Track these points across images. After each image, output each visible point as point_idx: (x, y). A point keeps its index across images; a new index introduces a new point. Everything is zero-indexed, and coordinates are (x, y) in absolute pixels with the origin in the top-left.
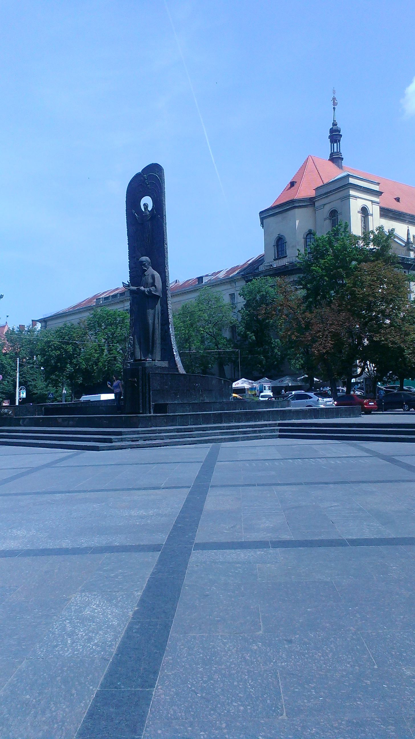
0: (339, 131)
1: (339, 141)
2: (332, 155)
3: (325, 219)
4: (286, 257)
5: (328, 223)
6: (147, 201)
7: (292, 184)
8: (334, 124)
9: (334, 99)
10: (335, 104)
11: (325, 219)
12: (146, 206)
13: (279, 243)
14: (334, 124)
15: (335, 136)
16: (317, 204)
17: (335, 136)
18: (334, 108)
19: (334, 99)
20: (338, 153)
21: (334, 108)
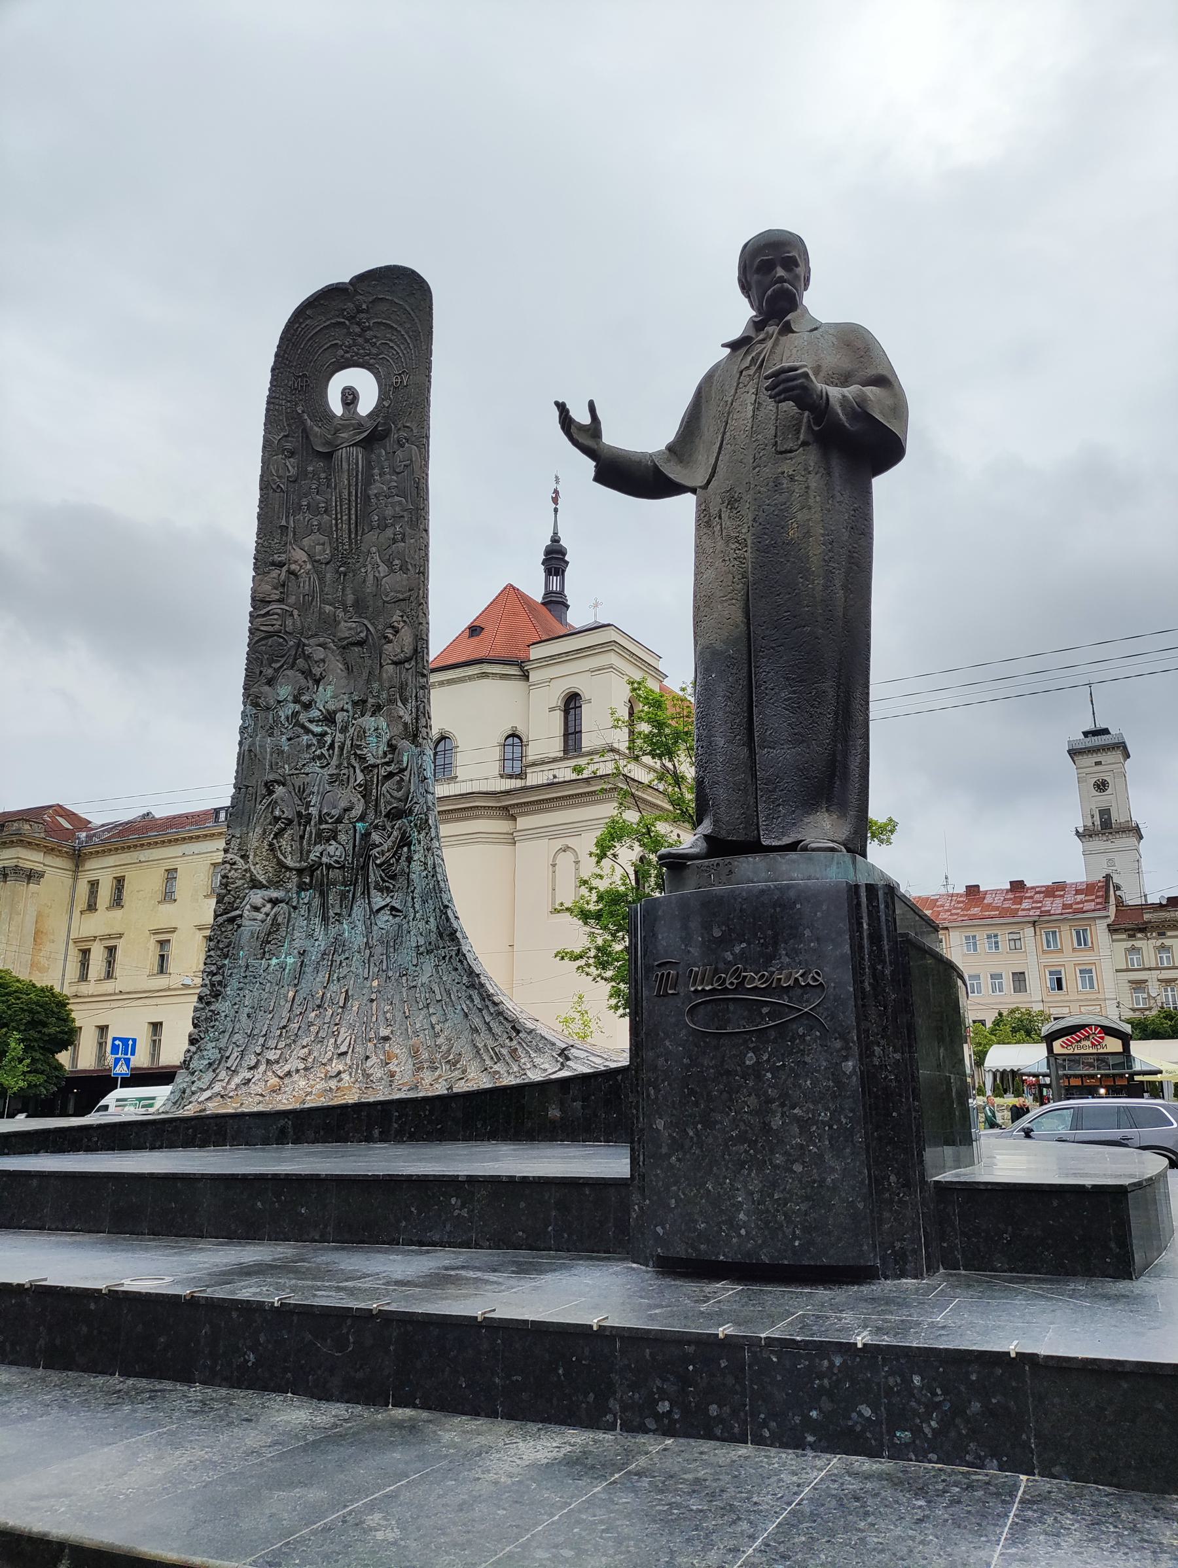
0: (564, 554)
1: (563, 571)
2: (548, 593)
3: (552, 709)
5: (559, 716)
6: (357, 387)
7: (474, 630)
8: (555, 540)
9: (556, 492)
10: (555, 500)
11: (552, 709)
12: (350, 397)
13: (441, 747)
14: (555, 540)
15: (555, 560)
16: (533, 676)
17: (555, 560)
18: (556, 510)
19: (556, 492)
20: (561, 593)
21: (556, 510)
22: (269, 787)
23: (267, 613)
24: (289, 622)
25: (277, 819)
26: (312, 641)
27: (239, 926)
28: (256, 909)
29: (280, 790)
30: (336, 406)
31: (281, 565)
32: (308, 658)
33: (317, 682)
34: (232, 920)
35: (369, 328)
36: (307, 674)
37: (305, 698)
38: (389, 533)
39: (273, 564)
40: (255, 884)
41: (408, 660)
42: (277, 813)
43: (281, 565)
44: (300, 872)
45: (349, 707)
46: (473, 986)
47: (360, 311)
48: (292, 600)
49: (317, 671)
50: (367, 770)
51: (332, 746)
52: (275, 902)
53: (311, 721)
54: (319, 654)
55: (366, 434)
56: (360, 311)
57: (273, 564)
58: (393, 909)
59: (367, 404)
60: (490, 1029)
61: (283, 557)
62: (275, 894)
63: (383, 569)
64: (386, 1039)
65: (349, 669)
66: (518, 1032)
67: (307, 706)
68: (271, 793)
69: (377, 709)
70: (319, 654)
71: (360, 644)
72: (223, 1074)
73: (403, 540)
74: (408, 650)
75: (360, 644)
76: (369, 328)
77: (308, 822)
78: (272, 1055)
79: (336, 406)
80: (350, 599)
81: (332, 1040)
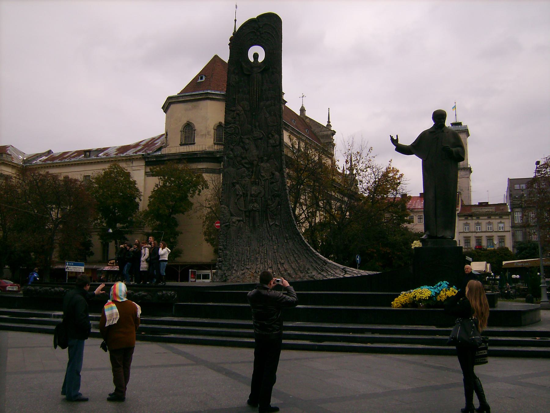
4: (194, 144)
6: (257, 52)
12: (256, 56)
22: (234, 185)
23: (230, 127)
24: (237, 130)
25: (237, 195)
26: (245, 137)
27: (229, 228)
28: (234, 223)
29: (237, 186)
30: (252, 60)
31: (234, 111)
32: (243, 142)
33: (246, 150)
34: (226, 226)
35: (263, 33)
36: (243, 148)
37: (243, 156)
38: (269, 102)
39: (231, 111)
40: (232, 215)
41: (277, 146)
42: (238, 193)
43: (234, 111)
44: (245, 212)
45: (257, 159)
46: (307, 250)
47: (260, 28)
48: (237, 123)
49: (247, 147)
50: (265, 180)
51: (252, 172)
52: (239, 221)
53: (245, 163)
54: (247, 141)
55: (261, 70)
56: (260, 28)
57: (231, 111)
58: (276, 225)
59: (261, 59)
60: (316, 262)
61: (234, 109)
62: (239, 219)
63: (268, 115)
64: (283, 264)
65: (257, 147)
66: (326, 264)
67: (245, 158)
68: (234, 186)
69: (267, 161)
70: (247, 141)
71: (261, 139)
72: (234, 272)
73: (274, 105)
74: (278, 143)
75: (261, 139)
76: (263, 33)
77: (247, 196)
78: (247, 267)
79: (252, 60)
80: (257, 124)
81: (266, 264)
